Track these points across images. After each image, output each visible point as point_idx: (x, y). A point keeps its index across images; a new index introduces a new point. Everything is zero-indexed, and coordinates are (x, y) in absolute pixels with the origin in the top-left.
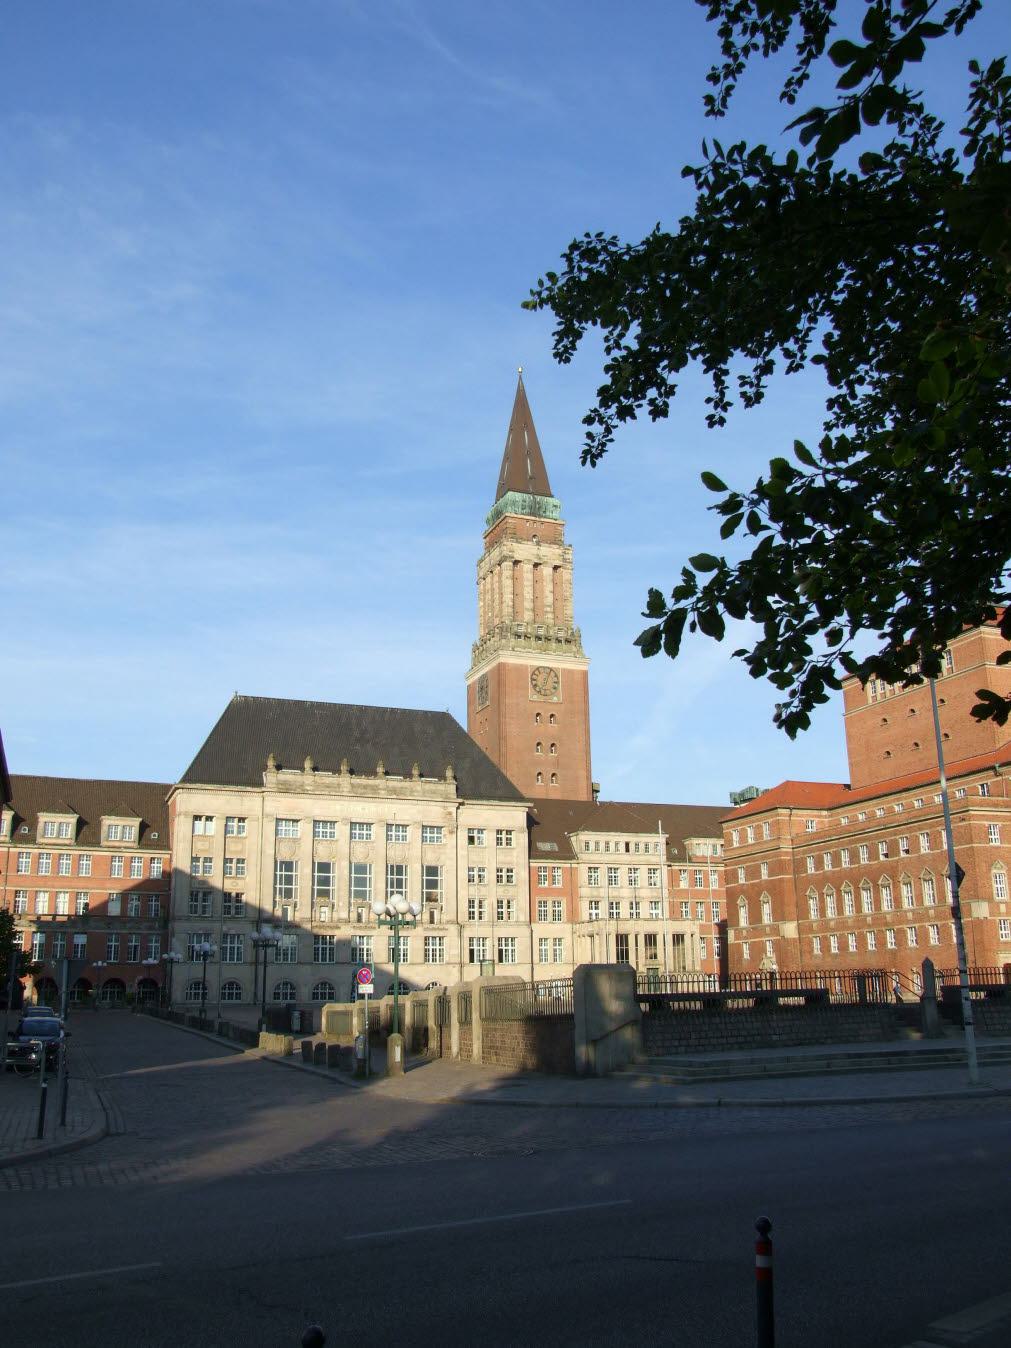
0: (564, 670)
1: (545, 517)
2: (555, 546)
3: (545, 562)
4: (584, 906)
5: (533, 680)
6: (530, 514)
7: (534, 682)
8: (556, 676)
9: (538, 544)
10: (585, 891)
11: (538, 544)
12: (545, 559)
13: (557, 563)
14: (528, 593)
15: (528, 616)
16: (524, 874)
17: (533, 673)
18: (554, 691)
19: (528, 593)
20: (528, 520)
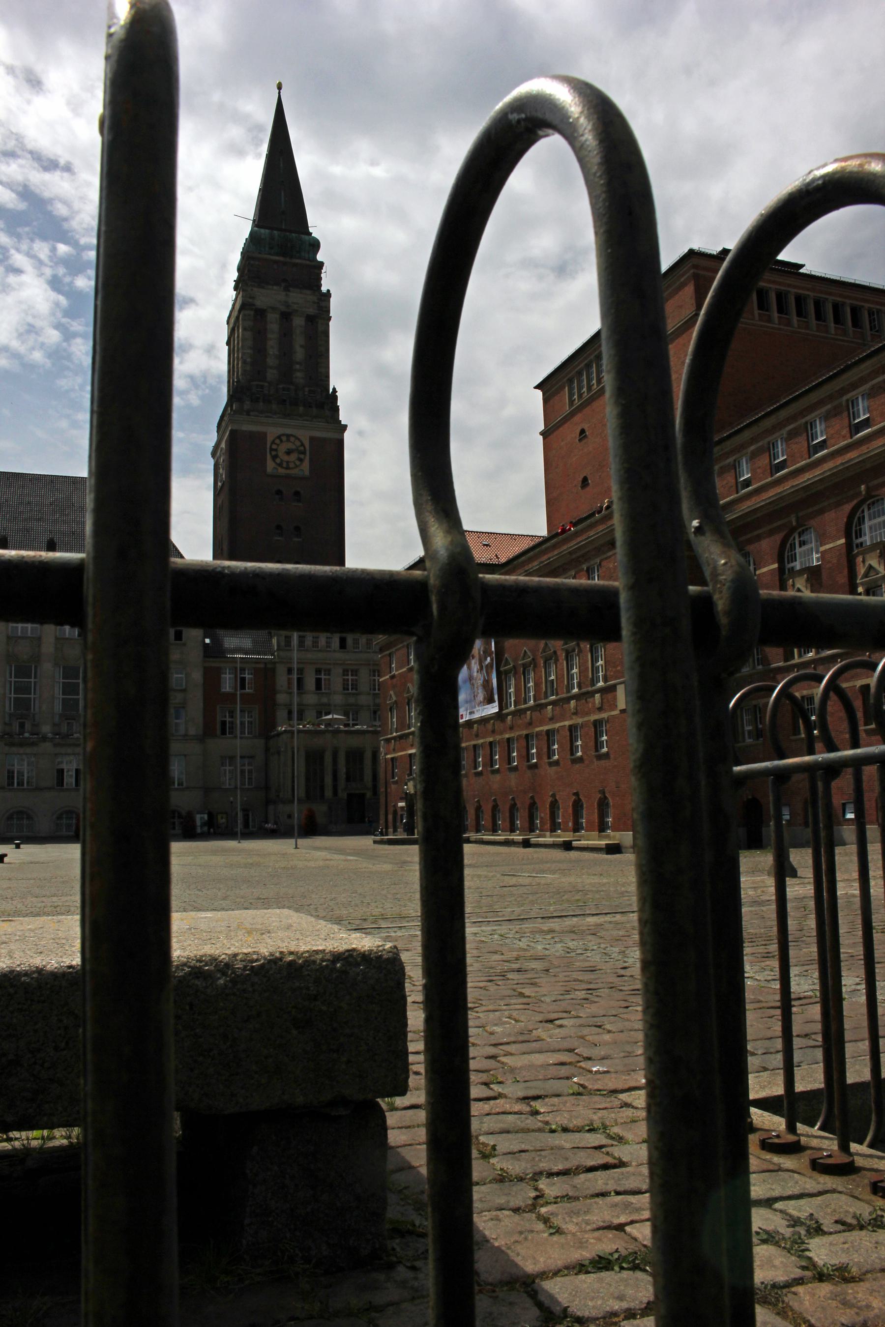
0: (312, 439)
1: (300, 258)
2: (308, 292)
3: (297, 311)
4: (282, 714)
5: (271, 450)
6: (277, 254)
7: (274, 453)
8: (302, 445)
9: (287, 289)
10: (281, 698)
11: (287, 289)
12: (295, 307)
13: (311, 311)
14: (272, 347)
15: (272, 374)
16: (197, 676)
17: (273, 442)
18: (298, 463)
19: (272, 347)
20: (276, 262)
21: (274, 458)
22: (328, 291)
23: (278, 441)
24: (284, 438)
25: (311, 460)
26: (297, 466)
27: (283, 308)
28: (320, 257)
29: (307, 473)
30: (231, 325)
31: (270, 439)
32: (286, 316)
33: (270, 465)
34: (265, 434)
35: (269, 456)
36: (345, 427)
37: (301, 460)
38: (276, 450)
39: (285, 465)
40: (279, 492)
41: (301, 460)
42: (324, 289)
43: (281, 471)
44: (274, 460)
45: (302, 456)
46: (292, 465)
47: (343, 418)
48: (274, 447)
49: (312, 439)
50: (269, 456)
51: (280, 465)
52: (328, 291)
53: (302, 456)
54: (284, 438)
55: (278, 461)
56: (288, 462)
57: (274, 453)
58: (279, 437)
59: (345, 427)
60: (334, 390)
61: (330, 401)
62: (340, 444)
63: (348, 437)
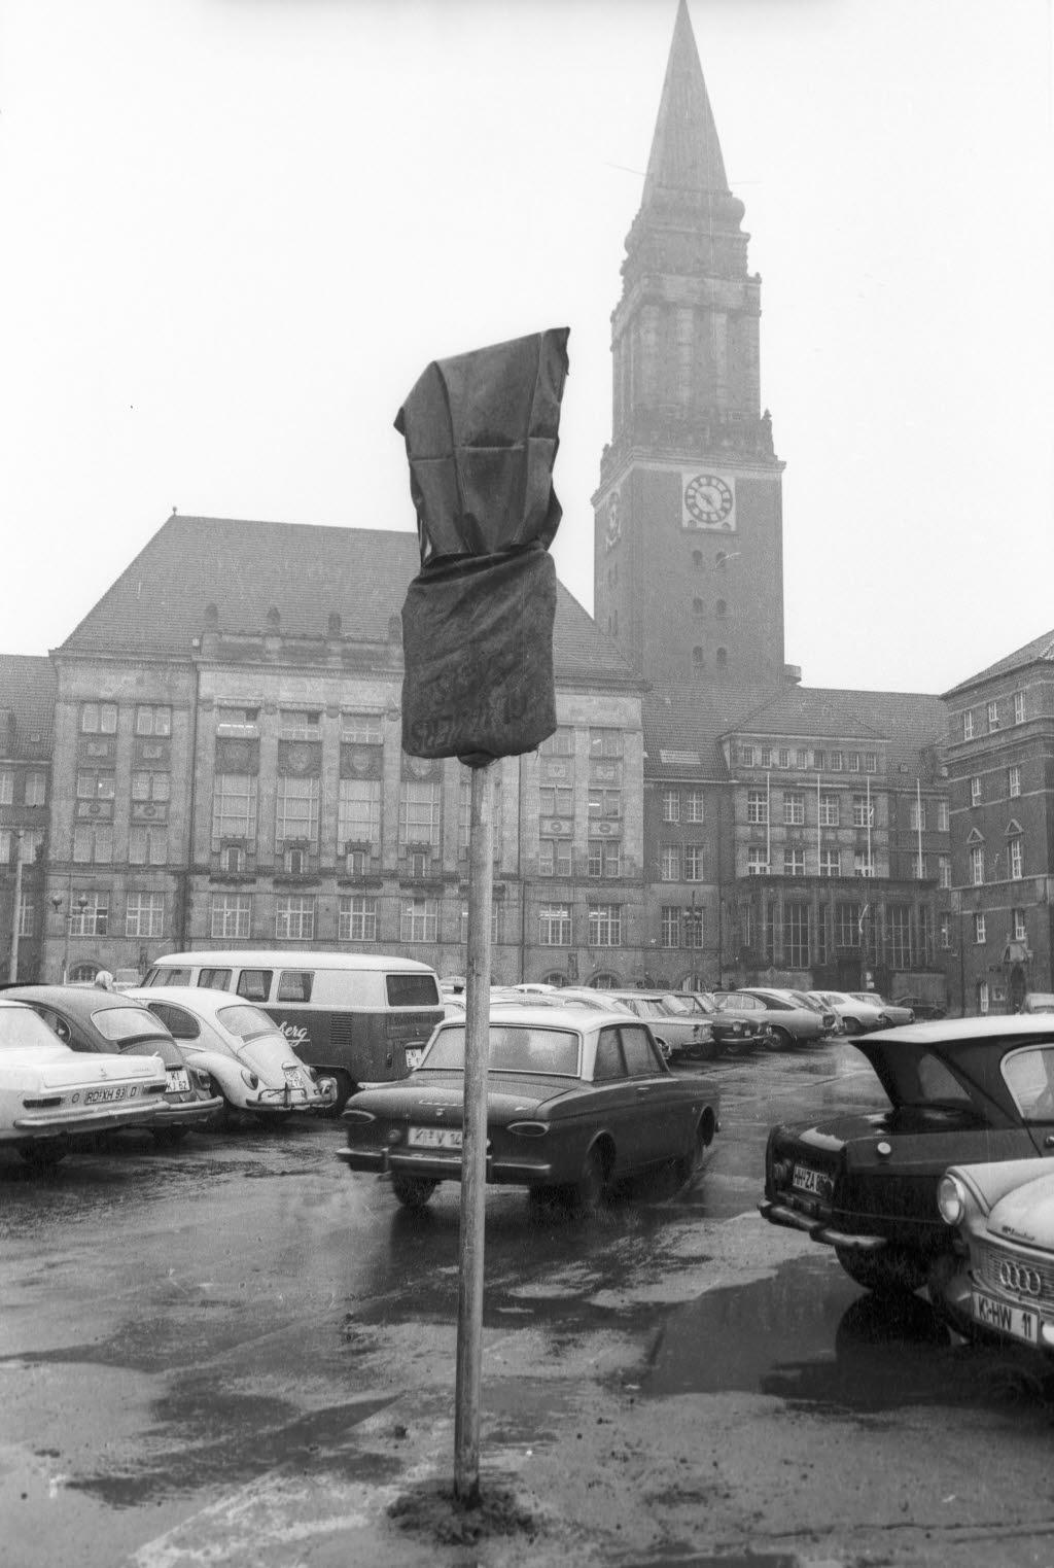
5: (687, 497)
7: (690, 501)
8: (728, 490)
10: (743, 832)
13: (734, 302)
17: (689, 487)
18: (722, 514)
21: (691, 507)
22: (758, 275)
23: (695, 485)
24: (703, 481)
25: (738, 514)
26: (720, 519)
27: (696, 300)
28: (744, 226)
29: (733, 529)
30: (620, 326)
31: (685, 485)
32: (702, 311)
33: (686, 516)
34: (679, 475)
35: (684, 506)
36: (784, 464)
37: (723, 509)
38: (694, 497)
39: (705, 516)
40: (697, 555)
41: (726, 511)
42: (751, 272)
43: (702, 525)
44: (691, 512)
45: (727, 505)
46: (714, 517)
47: (781, 450)
48: (691, 492)
49: (738, 481)
50: (684, 506)
51: (699, 517)
52: (758, 275)
53: (727, 505)
54: (703, 481)
55: (696, 511)
56: (708, 514)
57: (690, 501)
58: (697, 480)
59: (784, 464)
60: (767, 415)
61: (761, 430)
62: (776, 487)
63: (787, 479)
